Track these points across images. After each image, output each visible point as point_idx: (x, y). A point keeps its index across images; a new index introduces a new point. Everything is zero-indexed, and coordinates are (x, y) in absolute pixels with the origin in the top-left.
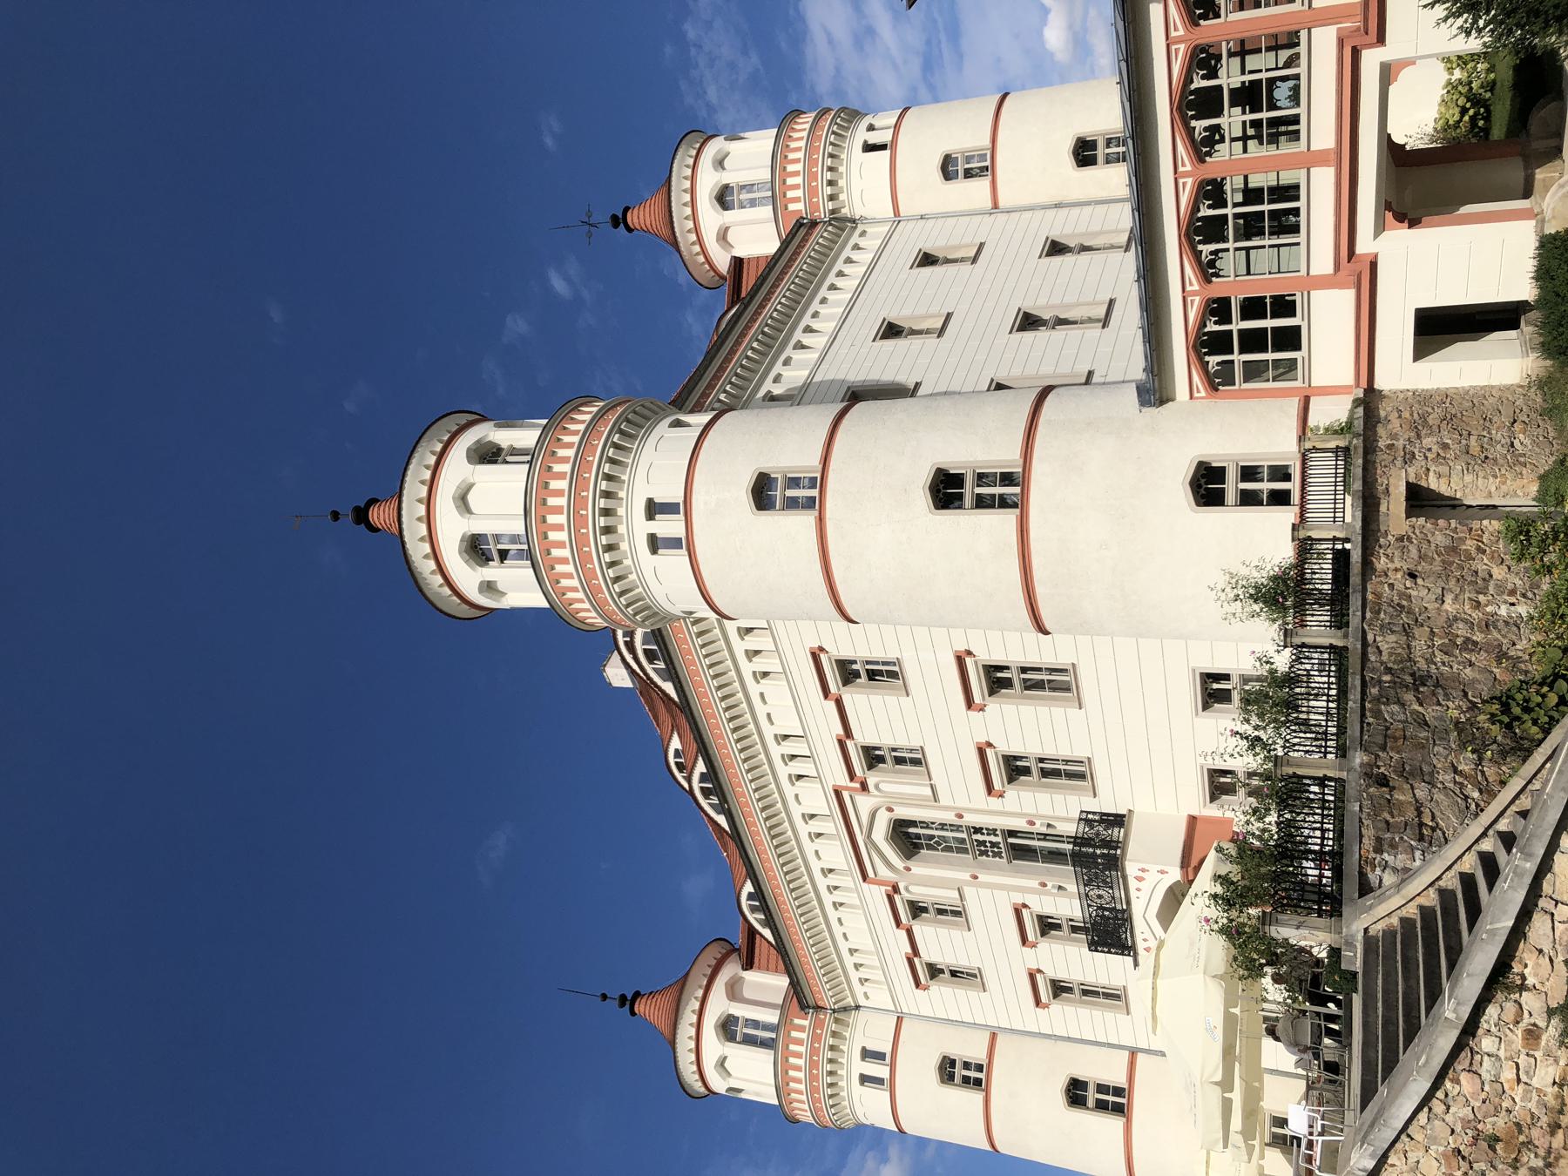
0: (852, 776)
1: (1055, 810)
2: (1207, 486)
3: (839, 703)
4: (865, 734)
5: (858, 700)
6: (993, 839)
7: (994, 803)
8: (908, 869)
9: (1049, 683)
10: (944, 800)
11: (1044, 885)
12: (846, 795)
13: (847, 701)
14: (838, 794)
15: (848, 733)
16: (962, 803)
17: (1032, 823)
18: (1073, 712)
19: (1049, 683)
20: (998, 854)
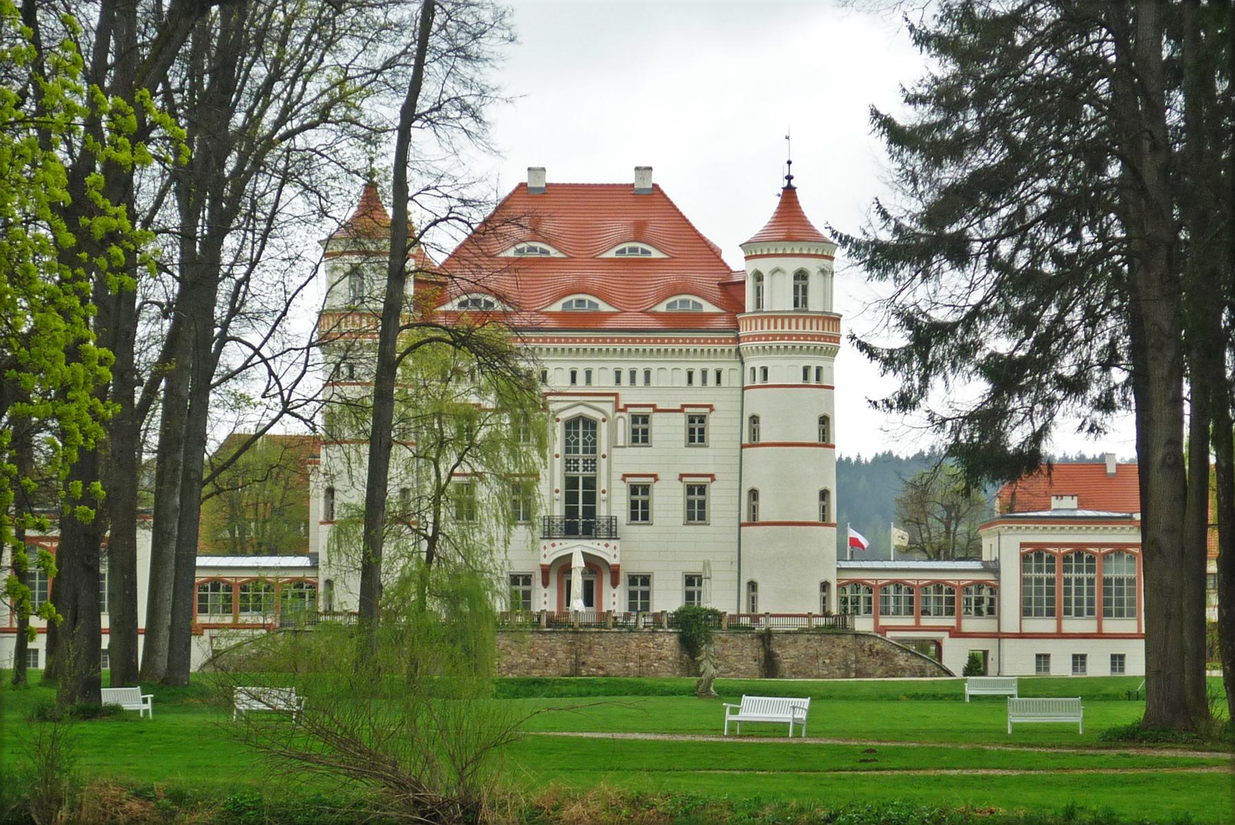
0: (627, 406)
1: (614, 503)
2: (825, 586)
3: (681, 411)
4: (657, 421)
5: (681, 421)
6: (581, 468)
7: (617, 476)
8: (558, 420)
9: (696, 511)
10: (615, 451)
11: (557, 491)
12: (613, 398)
13: (681, 415)
14: (616, 395)
15: (657, 411)
16: (614, 460)
17: (604, 492)
18: (682, 521)
19: (696, 511)
20: (568, 469)
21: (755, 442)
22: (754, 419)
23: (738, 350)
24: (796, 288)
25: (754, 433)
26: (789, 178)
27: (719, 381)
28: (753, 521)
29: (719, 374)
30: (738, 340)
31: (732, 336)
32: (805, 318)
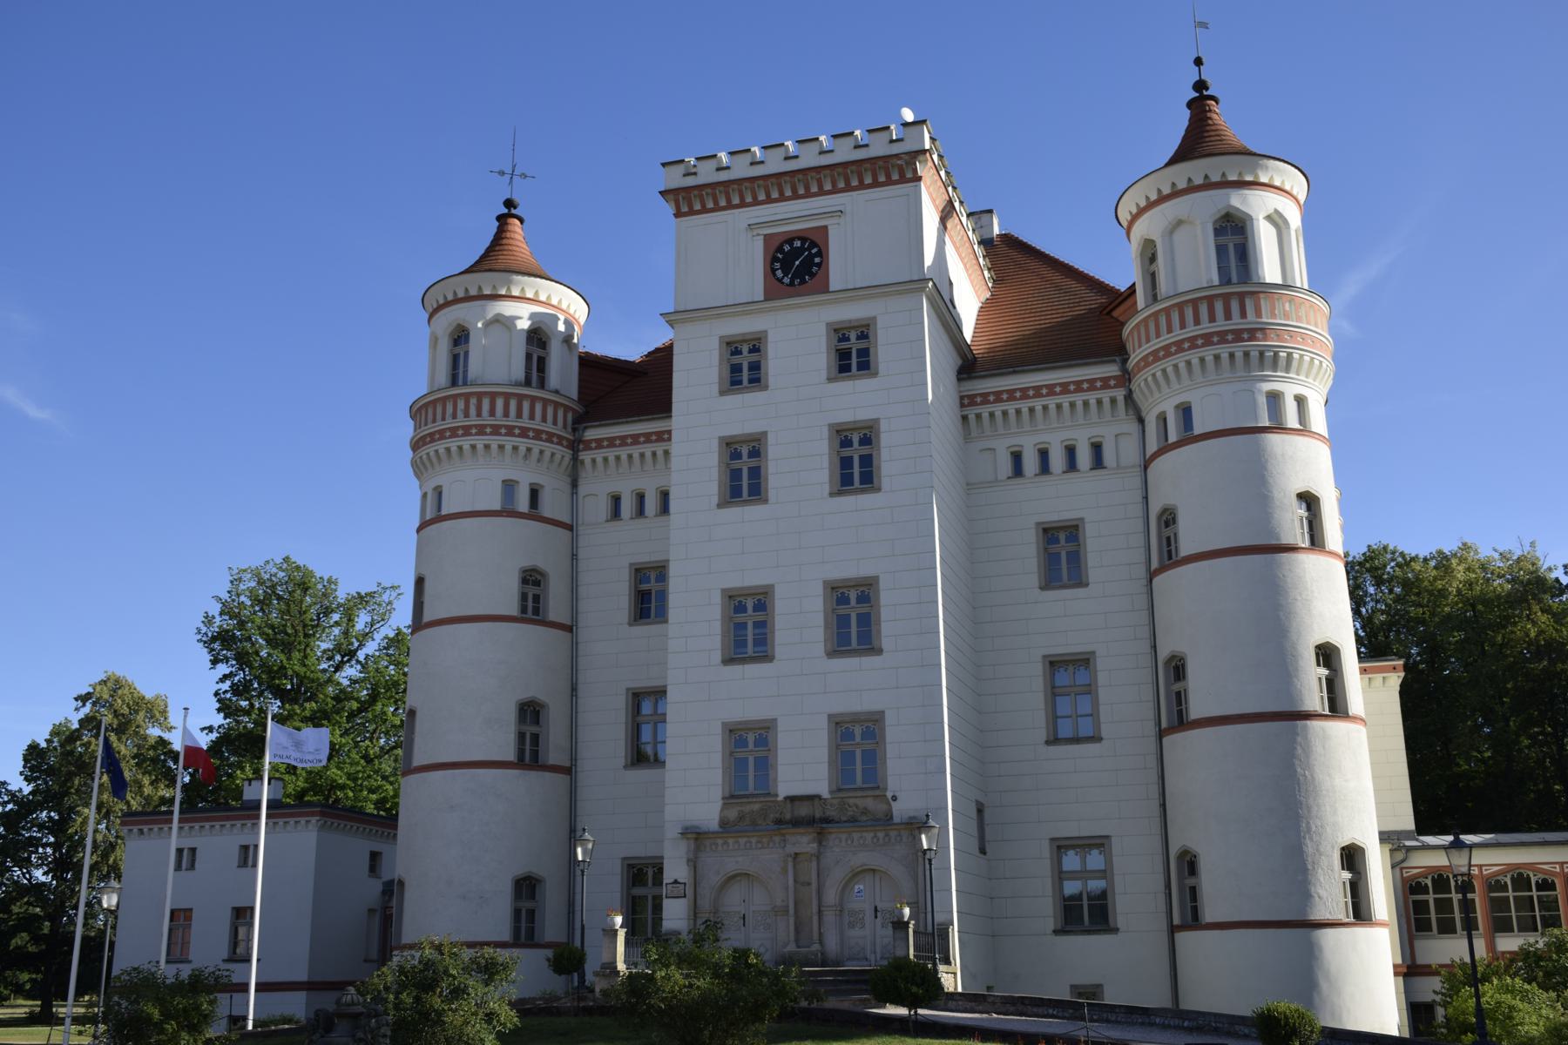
21: (1170, 557)
22: (1169, 518)
23: (1129, 397)
24: (1221, 251)
25: (1169, 545)
26: (1200, 85)
27: (1098, 462)
28: (1181, 722)
29: (1097, 448)
30: (1125, 378)
31: (1111, 370)
32: (1242, 297)
